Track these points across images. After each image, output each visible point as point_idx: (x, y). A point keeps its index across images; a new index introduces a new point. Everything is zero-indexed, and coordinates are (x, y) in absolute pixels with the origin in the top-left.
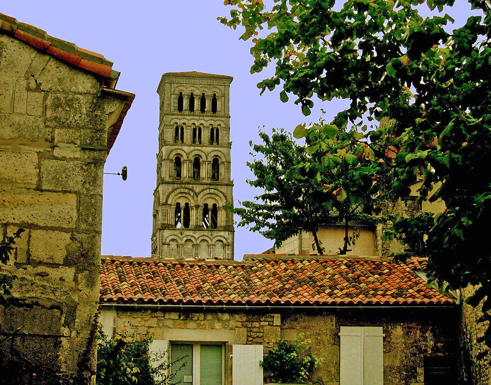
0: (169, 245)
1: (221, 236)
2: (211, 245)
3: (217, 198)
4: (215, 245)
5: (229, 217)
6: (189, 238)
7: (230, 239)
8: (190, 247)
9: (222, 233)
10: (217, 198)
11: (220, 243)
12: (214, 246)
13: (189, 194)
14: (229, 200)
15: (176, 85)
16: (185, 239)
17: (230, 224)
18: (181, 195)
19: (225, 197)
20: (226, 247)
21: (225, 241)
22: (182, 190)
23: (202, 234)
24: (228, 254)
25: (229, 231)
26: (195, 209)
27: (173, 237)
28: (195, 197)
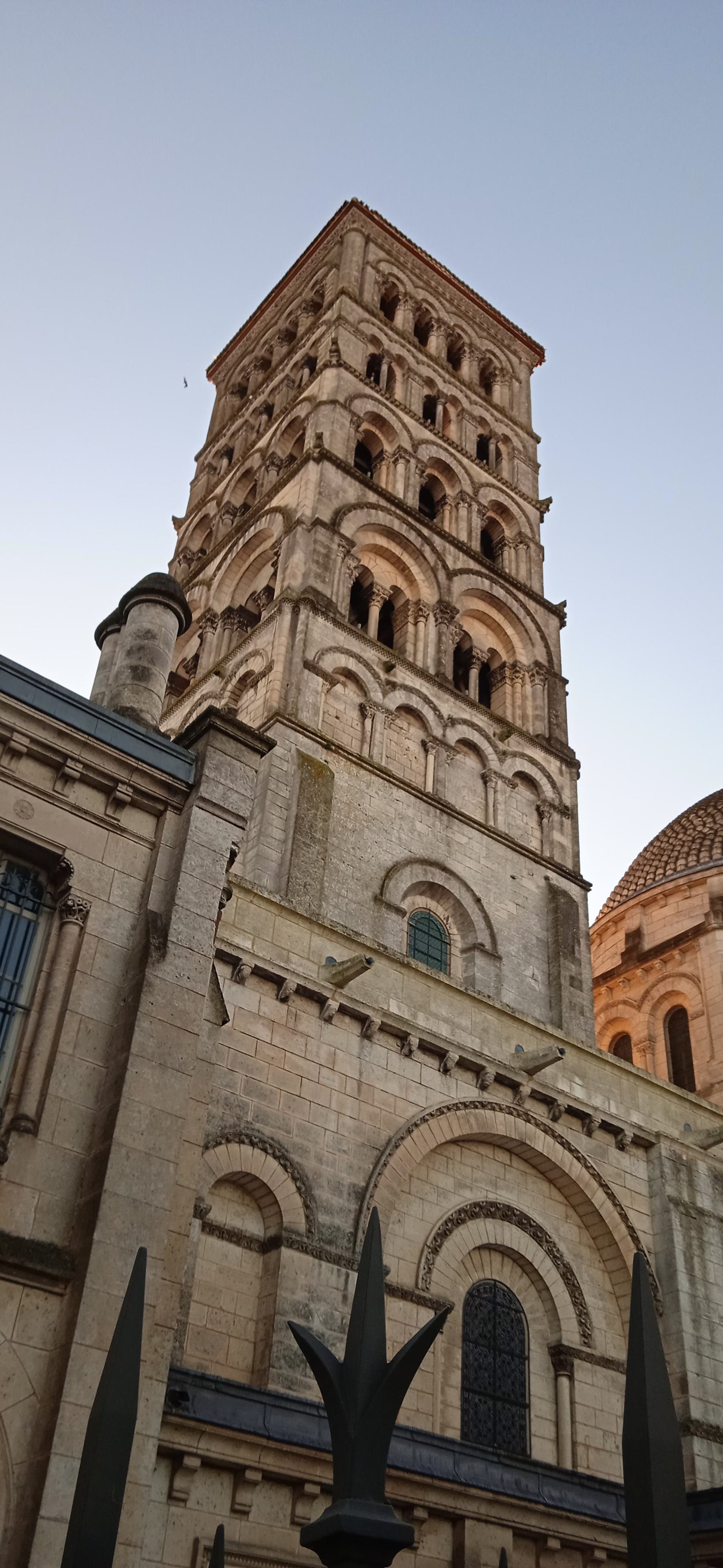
0: (330, 679)
4: (514, 786)
6: (415, 702)
8: (415, 748)
9: (538, 755)
13: (418, 554)
15: (382, 255)
16: (398, 698)
18: (382, 541)
20: (556, 817)
21: (548, 792)
22: (396, 525)
23: (466, 716)
26: (432, 619)
27: (352, 664)
28: (442, 575)
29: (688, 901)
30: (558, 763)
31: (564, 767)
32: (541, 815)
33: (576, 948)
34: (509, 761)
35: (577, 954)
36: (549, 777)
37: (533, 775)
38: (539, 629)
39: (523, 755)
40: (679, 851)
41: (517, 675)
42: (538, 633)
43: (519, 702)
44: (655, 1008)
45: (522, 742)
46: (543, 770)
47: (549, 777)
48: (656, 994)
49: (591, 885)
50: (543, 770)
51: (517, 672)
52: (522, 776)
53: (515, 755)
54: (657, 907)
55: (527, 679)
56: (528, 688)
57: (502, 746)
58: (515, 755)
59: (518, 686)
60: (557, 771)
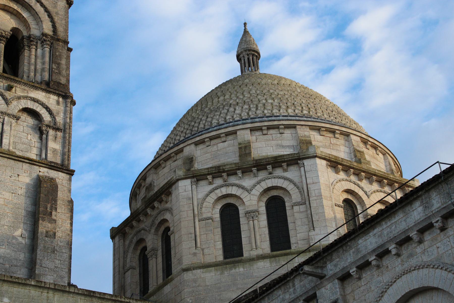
1: (35, 100)
2: (9, 115)
3: (25, 15)
4: (18, 118)
5: (59, 64)
7: (62, 115)
9: (40, 95)
10: (25, 15)
11: (30, 121)
12: (14, 121)
14: (60, 29)
17: (63, 81)
19: (50, 16)
20: (51, 132)
21: (46, 117)
24: (54, 151)
25: (59, 95)
29: (176, 162)
30: (56, 98)
31: (61, 99)
32: (41, 133)
33: (54, 213)
34: (15, 103)
35: (54, 217)
36: (47, 108)
37: (35, 108)
38: (46, 10)
39: (26, 98)
40: (193, 126)
41: (32, 43)
42: (46, 14)
43: (33, 61)
44: (157, 230)
45: (26, 88)
46: (43, 105)
47: (47, 108)
48: (157, 222)
49: (75, 171)
50: (43, 105)
51: (32, 41)
52: (27, 110)
53: (19, 98)
54: (161, 168)
55: (39, 45)
56: (39, 51)
57: (8, 94)
58: (19, 98)
59: (33, 50)
60: (54, 102)
